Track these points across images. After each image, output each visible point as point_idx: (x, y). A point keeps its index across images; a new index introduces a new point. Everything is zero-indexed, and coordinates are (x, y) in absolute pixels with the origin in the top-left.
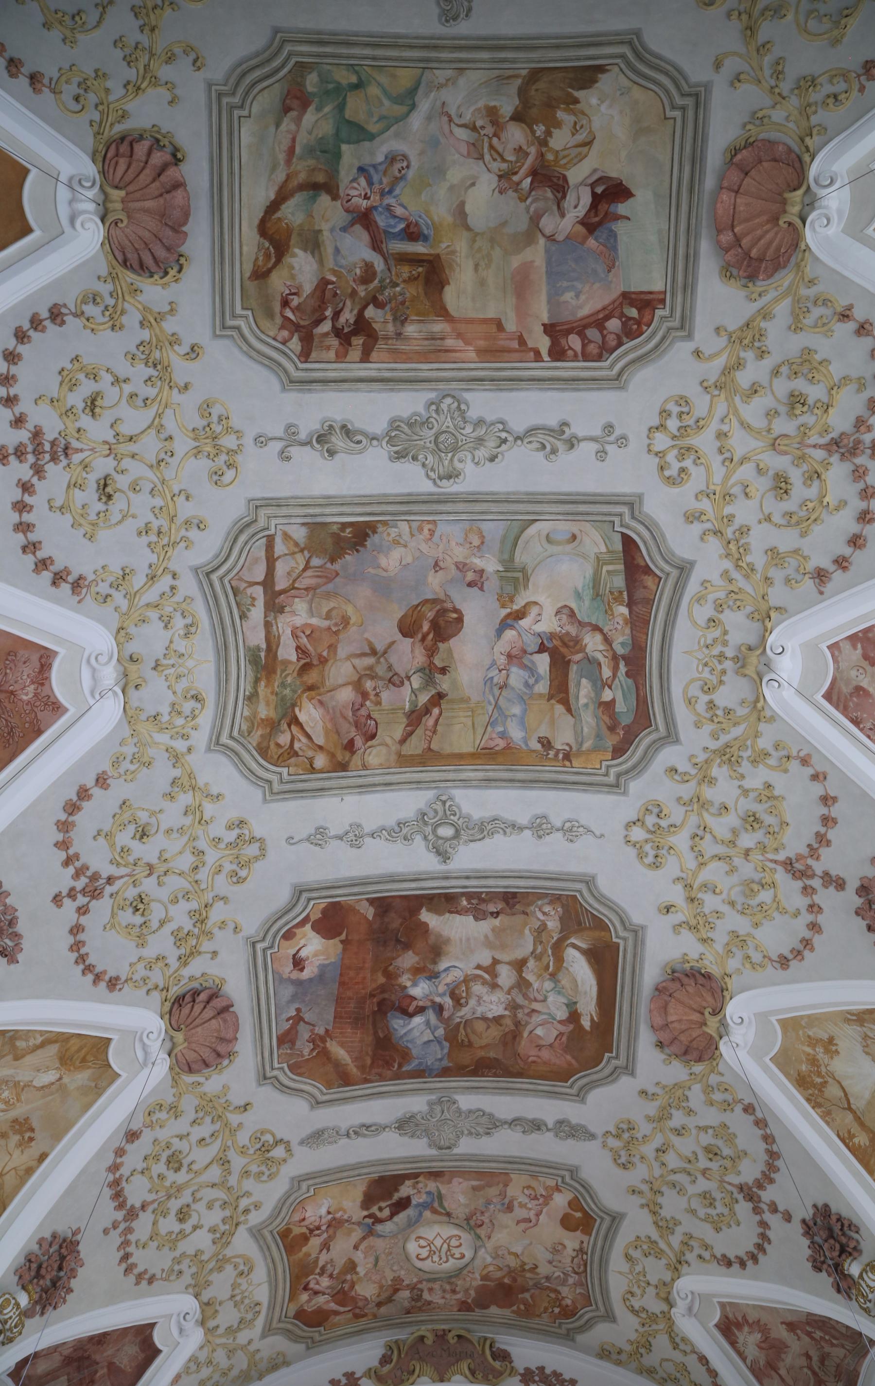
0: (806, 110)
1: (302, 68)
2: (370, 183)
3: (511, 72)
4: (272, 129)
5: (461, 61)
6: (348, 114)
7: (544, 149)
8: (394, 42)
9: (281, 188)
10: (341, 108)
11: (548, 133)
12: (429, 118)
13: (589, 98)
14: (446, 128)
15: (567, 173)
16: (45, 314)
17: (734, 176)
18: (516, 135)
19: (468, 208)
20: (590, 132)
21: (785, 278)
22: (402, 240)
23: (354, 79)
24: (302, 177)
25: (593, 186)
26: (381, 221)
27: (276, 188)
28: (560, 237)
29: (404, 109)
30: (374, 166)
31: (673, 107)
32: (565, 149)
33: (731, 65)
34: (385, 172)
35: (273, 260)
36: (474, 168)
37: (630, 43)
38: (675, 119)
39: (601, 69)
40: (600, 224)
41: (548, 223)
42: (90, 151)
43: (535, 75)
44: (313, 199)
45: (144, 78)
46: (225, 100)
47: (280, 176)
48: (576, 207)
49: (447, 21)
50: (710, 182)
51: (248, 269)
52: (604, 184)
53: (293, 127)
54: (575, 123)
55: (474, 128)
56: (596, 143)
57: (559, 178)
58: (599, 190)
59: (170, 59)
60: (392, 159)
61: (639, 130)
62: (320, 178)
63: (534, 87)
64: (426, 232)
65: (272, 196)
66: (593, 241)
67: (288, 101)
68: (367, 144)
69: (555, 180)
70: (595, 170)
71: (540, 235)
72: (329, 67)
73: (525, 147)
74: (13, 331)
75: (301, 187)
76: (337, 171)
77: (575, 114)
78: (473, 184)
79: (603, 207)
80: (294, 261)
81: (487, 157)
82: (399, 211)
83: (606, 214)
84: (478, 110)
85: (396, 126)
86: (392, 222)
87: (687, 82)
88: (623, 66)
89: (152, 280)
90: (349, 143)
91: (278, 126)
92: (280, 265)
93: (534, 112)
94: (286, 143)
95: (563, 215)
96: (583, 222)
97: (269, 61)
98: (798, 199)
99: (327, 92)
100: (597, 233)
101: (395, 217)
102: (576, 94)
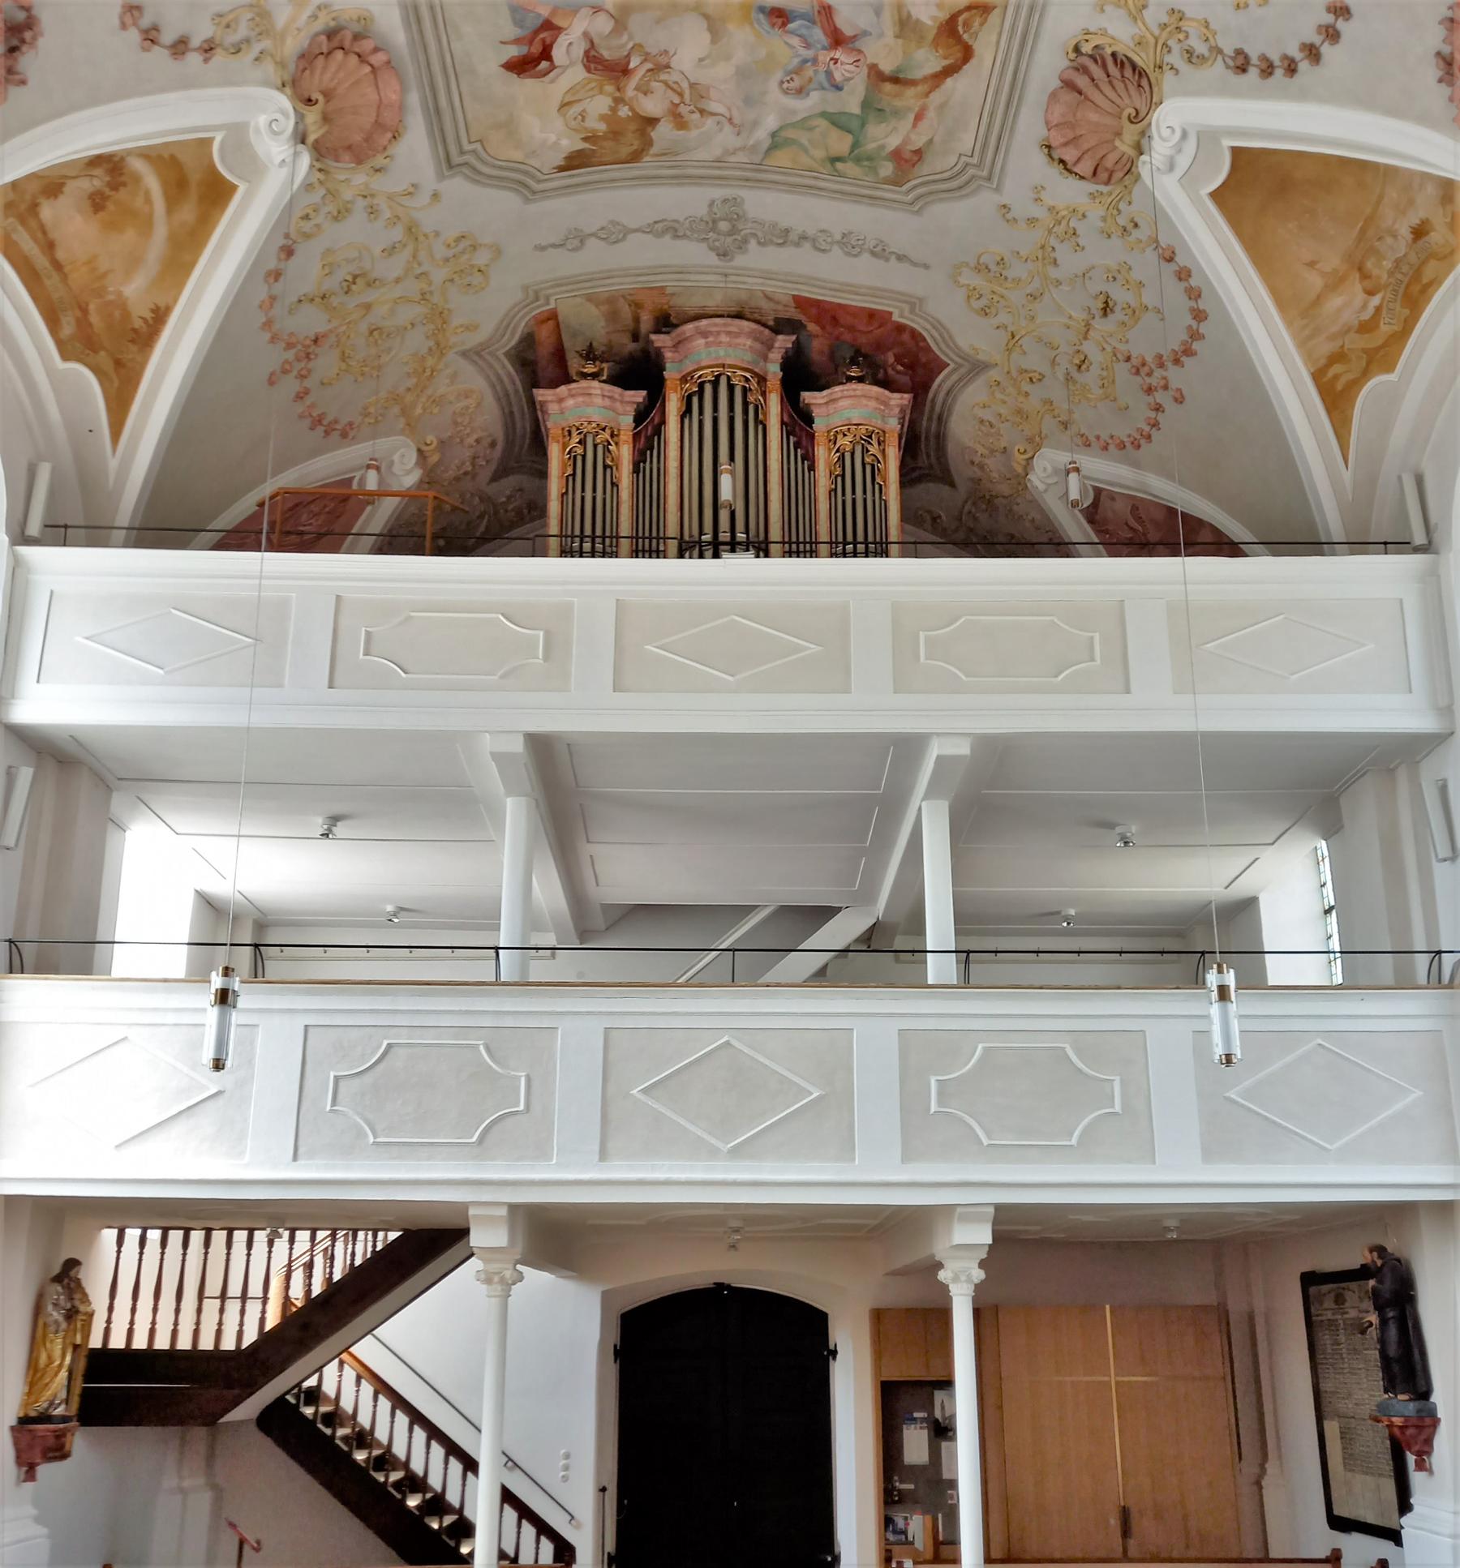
0: (332, 194)
1: (897, 181)
2: (829, 74)
3: (663, 158)
4: (937, 139)
5: (719, 168)
6: (849, 139)
7: (618, 94)
8: (793, 188)
9: (937, 86)
10: (855, 145)
11: (614, 110)
12: (755, 124)
13: (571, 143)
14: (735, 114)
15: (586, 75)
16: (1253, 72)
17: (388, 117)
18: (651, 106)
19: (707, 37)
20: (564, 116)
21: (293, 46)
22: (793, 11)
23: (839, 165)
24: (911, 92)
25: (553, 67)
26: (818, 35)
27: (943, 87)
28: (585, 11)
29: (783, 134)
30: (823, 88)
31: (474, 151)
32: (592, 97)
33: (424, 198)
34: (810, 80)
35: (961, 19)
36: (702, 76)
37: (534, 193)
38: (470, 142)
39: (561, 169)
40: (537, 32)
41: (602, 25)
42: (1138, 183)
43: (635, 157)
44: (899, 70)
45: (1063, 217)
46: (985, 173)
47: (936, 97)
48: (570, 44)
49: (735, 199)
50: (414, 99)
51: (994, 18)
52: (540, 71)
53: (913, 137)
54: (583, 121)
55: (702, 112)
56: (556, 104)
57: (596, 69)
58: (544, 64)
59: (1032, 221)
60: (800, 92)
61: (509, 127)
62: (888, 87)
63: (635, 147)
64: (761, 16)
65: (949, 81)
66: (542, 12)
67: (916, 158)
68: (831, 110)
69: (600, 67)
70: (552, 81)
71: (612, 11)
72: (867, 179)
73: (641, 95)
74: (1297, 76)
75: (912, 83)
76: (867, 89)
77: (586, 129)
78: (701, 60)
79: (536, 49)
80: (935, 12)
81: (685, 85)
82: (795, 41)
83: (531, 42)
84: (697, 127)
85: (794, 120)
86: (804, 31)
87: (465, 174)
88: (539, 174)
89: (1118, 48)
90: (852, 114)
91: (931, 141)
92: (952, 13)
93: (633, 127)
94: (924, 125)
95: (586, 34)
96: (558, 30)
97: (931, 193)
98: (311, 128)
99: (870, 159)
100: (539, 22)
101: (799, 36)
102: (586, 145)
